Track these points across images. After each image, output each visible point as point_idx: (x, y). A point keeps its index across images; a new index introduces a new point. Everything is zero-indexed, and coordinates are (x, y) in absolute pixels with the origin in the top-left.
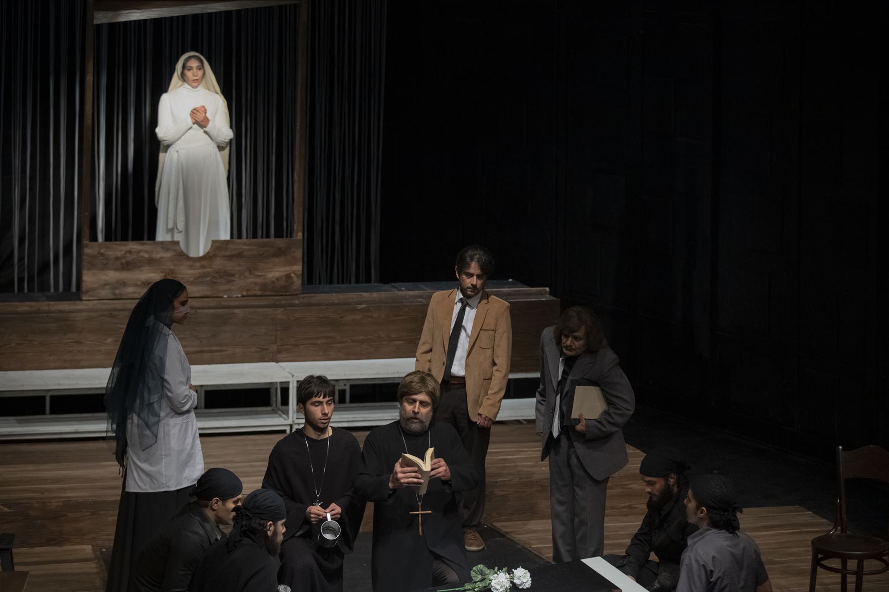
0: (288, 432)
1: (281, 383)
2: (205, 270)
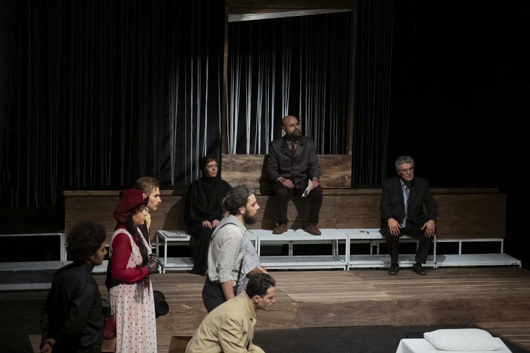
0: (345, 269)
1: (339, 240)
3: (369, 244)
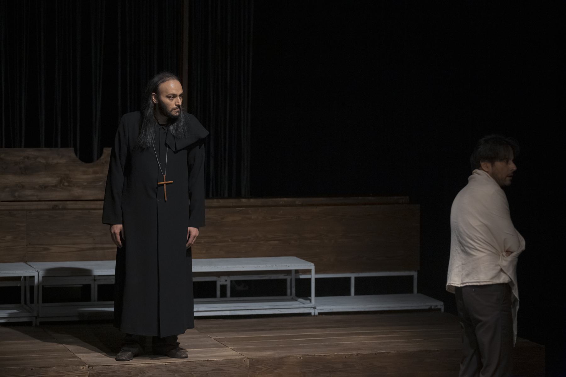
2: (98, 175)
3: (214, 283)
